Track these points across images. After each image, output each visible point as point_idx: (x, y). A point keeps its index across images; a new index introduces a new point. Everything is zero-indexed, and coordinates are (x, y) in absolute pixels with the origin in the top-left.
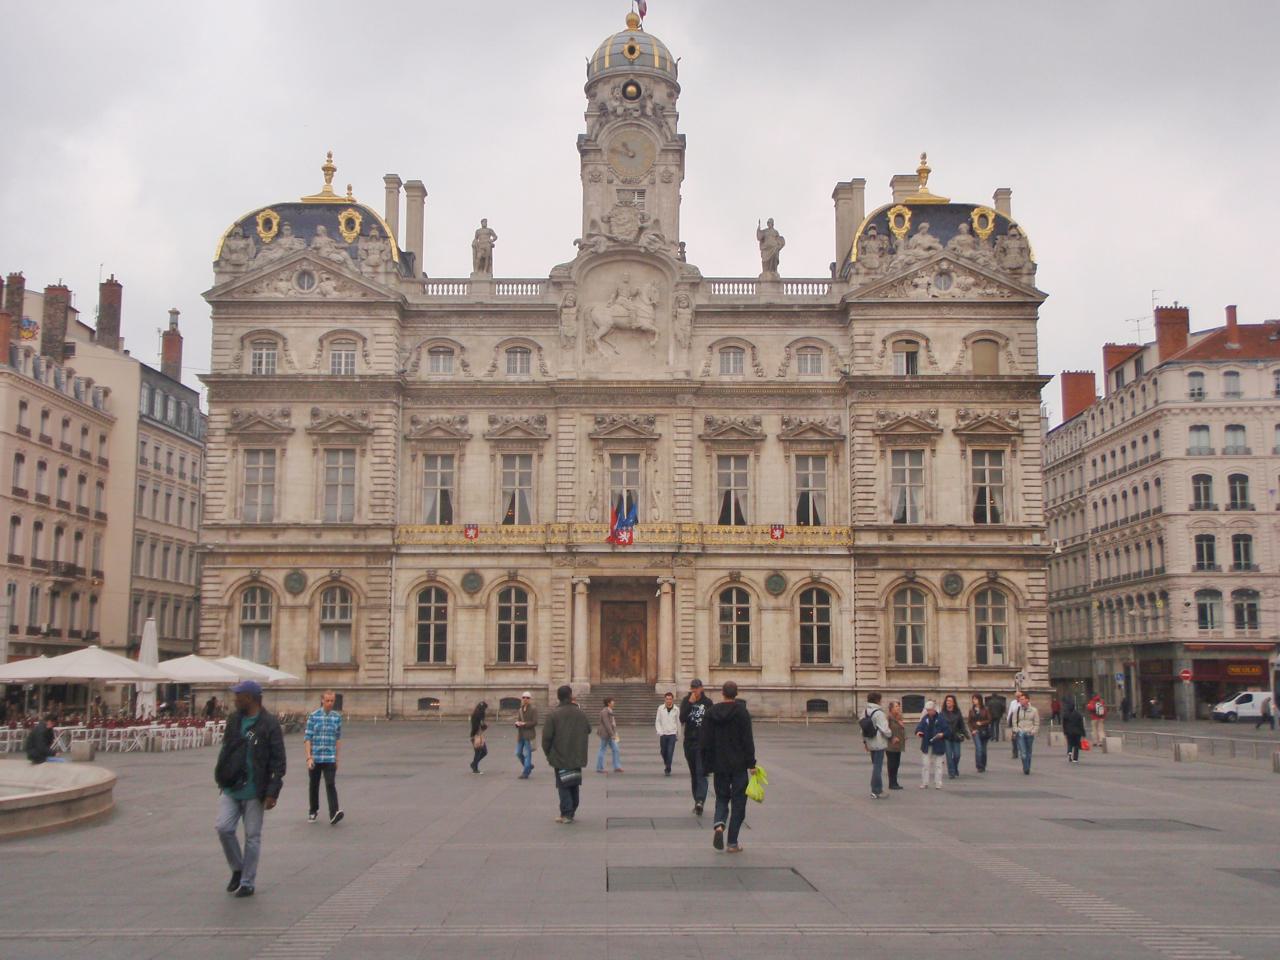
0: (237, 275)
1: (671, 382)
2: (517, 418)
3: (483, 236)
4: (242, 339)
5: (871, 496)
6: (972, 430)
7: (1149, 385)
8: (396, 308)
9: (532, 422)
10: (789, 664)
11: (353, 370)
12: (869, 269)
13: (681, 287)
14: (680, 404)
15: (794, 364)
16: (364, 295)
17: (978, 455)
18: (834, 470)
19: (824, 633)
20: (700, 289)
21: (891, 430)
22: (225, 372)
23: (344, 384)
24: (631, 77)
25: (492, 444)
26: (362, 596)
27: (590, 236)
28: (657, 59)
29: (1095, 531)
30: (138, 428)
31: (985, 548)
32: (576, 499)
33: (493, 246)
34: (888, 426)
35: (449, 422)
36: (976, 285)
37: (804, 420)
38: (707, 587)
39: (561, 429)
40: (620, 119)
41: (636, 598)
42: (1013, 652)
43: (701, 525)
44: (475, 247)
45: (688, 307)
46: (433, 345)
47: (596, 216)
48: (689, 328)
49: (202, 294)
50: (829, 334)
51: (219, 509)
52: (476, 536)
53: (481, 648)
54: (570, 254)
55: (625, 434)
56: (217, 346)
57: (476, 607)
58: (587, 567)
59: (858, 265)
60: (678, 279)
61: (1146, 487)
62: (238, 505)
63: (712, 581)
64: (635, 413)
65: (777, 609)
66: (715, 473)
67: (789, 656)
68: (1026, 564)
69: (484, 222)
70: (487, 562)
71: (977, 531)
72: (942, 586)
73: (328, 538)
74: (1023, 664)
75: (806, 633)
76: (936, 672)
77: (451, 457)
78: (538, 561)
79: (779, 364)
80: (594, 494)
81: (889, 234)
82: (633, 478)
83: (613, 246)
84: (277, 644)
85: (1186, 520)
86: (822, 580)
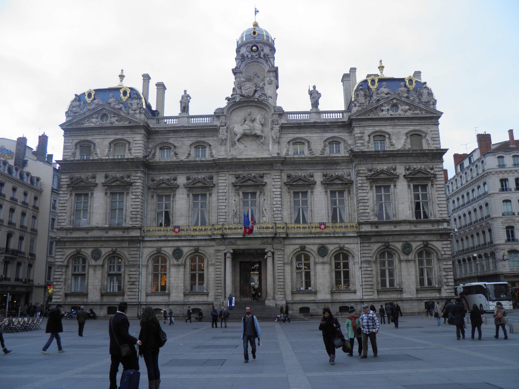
1: (270, 158)
2: (199, 177)
4: (76, 144)
5: (367, 208)
6: (412, 175)
7: (480, 164)
8: (144, 129)
10: (330, 289)
13: (274, 116)
14: (275, 169)
15: (328, 149)
17: (416, 187)
18: (348, 196)
19: (347, 274)
20: (283, 117)
21: (375, 176)
22: (67, 159)
24: (254, 43)
25: (188, 189)
26: (127, 262)
27: (232, 95)
28: (265, 36)
30: (52, 194)
31: (422, 230)
32: (227, 214)
33: (189, 102)
34: (373, 174)
35: (168, 180)
36: (409, 109)
37: (333, 174)
39: (219, 181)
42: (437, 280)
43: (286, 223)
44: (181, 102)
45: (278, 124)
46: (162, 146)
48: (278, 134)
49: (60, 126)
50: (343, 135)
51: (63, 221)
52: (179, 231)
53: (182, 284)
54: (224, 104)
55: (250, 183)
56: (65, 148)
57: (179, 265)
58: (232, 245)
59: (355, 102)
61: (481, 207)
62: (72, 219)
63: (292, 250)
64: (253, 173)
65: (323, 263)
66: (292, 199)
67: (330, 285)
68: (441, 238)
69: (185, 91)
72: (402, 250)
73: (111, 234)
74: (442, 286)
75: (338, 274)
76: (400, 291)
77: (170, 196)
78: (209, 243)
79: (321, 149)
80: (235, 211)
81: (369, 88)
82: (254, 204)
83: (242, 99)
84: (88, 283)
85: (501, 220)
86: (345, 248)
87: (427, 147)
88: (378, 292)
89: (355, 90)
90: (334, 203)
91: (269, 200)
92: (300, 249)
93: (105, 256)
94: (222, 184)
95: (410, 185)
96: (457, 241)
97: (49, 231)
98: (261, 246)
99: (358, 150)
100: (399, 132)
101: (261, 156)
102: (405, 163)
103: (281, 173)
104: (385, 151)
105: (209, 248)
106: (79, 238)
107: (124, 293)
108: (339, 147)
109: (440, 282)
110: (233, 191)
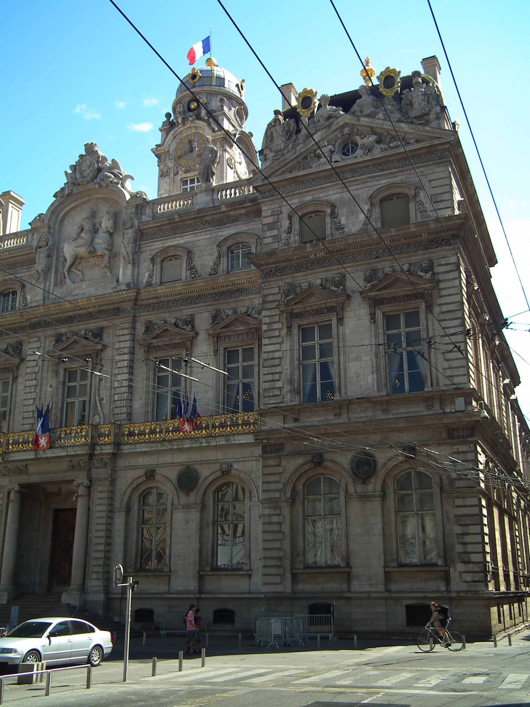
5: (277, 377)
10: (197, 568)
12: (276, 152)
15: (224, 260)
36: (379, 142)
37: (230, 312)
63: (129, 481)
65: (187, 507)
79: (212, 264)
95: (375, 314)
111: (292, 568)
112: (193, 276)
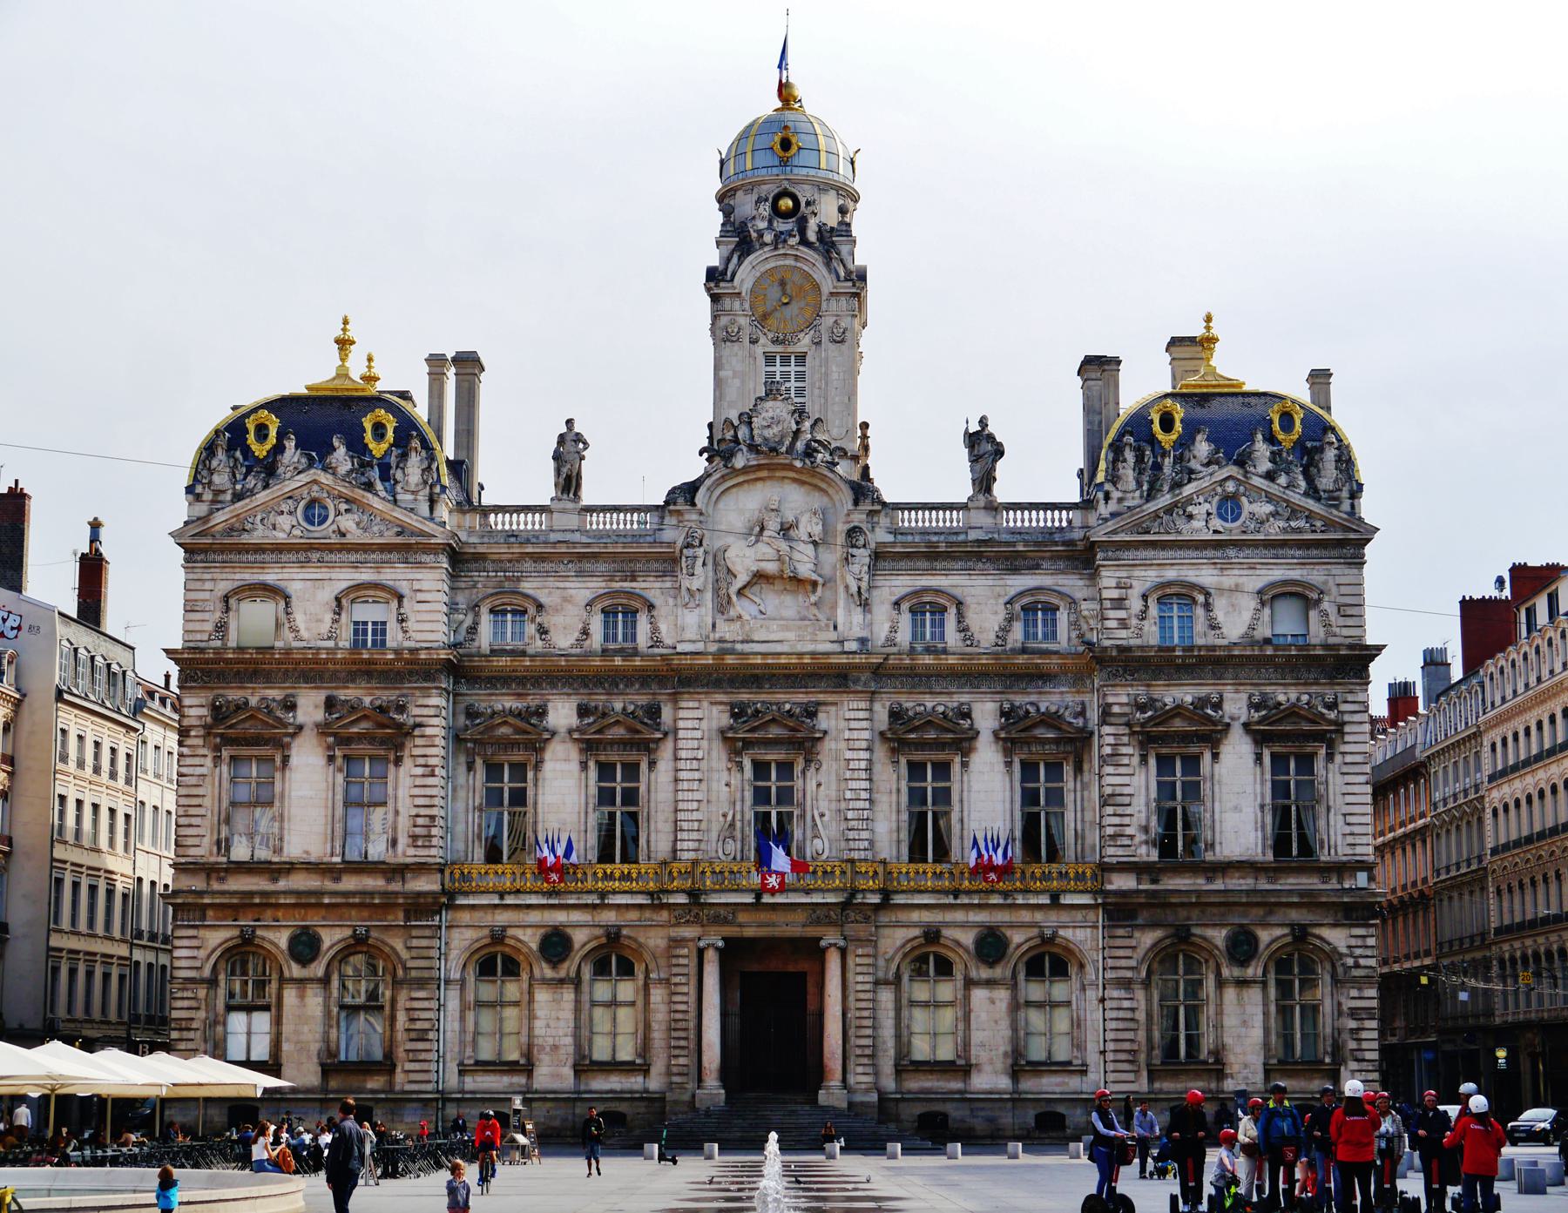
0: (219, 506)
3: (569, 446)
4: (226, 598)
5: (1126, 820)
9: (640, 713)
10: (1009, 1061)
11: (383, 642)
13: (853, 517)
16: (399, 534)
17: (1279, 762)
20: (884, 521)
21: (1155, 725)
22: (202, 645)
23: (370, 662)
24: (786, 184)
26: (400, 973)
29: (1494, 851)
32: (704, 826)
33: (582, 458)
34: (1151, 718)
35: (520, 714)
36: (1275, 514)
37: (1032, 709)
38: (891, 952)
40: (767, 249)
41: (791, 968)
42: (1329, 1042)
43: (884, 862)
44: (557, 457)
45: (864, 546)
47: (733, 416)
48: (866, 578)
50: (1073, 584)
53: (569, 1040)
54: (696, 467)
55: (774, 732)
56: (190, 608)
57: (562, 981)
59: (1108, 487)
60: (850, 506)
62: (223, 835)
63: (898, 943)
64: (791, 699)
65: (990, 983)
67: (1009, 1049)
69: (569, 422)
70: (576, 916)
71: (1275, 870)
73: (350, 883)
74: (1344, 1061)
78: (648, 914)
79: (997, 628)
80: (729, 818)
81: (1152, 440)
82: (786, 796)
86: (1058, 940)
87: (1322, 634)
88: (1150, 1072)
89: (1111, 445)
90: (1030, 797)
91: (834, 786)
92: (922, 940)
93: (332, 952)
94: (690, 734)
96: (1499, 892)
97: (52, 841)
98: (809, 929)
99: (1107, 643)
100: (1237, 589)
101: (810, 647)
102: (1252, 684)
103: (872, 701)
104: (1191, 648)
105: (652, 932)
106: (251, 894)
107: (394, 1066)
108: (1054, 621)
109: (1337, 1050)
110: (724, 756)
111: (1148, 1065)
112: (969, 642)
